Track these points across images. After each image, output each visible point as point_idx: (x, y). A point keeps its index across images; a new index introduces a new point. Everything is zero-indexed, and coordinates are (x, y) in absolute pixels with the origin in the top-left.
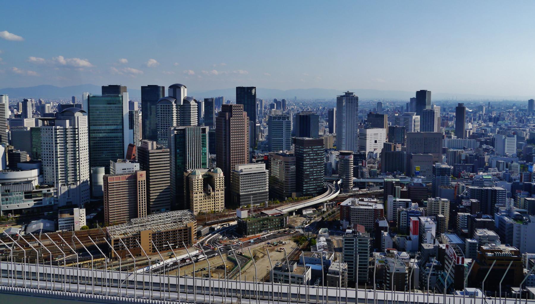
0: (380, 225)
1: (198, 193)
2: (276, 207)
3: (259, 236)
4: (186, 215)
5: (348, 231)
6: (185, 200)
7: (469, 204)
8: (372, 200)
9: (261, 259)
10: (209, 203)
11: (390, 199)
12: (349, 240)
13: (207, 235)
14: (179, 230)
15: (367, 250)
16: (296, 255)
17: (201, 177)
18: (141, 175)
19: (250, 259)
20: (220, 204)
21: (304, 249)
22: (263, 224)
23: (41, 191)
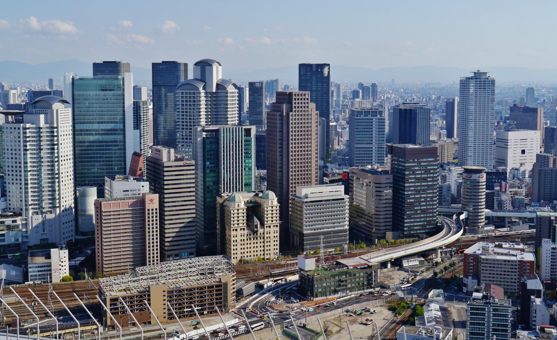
0: (529, 287)
2: (361, 254)
3: (333, 299)
4: (220, 264)
5: (475, 294)
6: (219, 240)
8: (516, 247)
9: (337, 336)
10: (255, 245)
12: (478, 309)
13: (251, 295)
14: (209, 287)
15: (506, 326)
16: (392, 330)
17: (242, 205)
18: (151, 201)
19: (318, 334)
20: (272, 248)
21: (404, 323)
22: (340, 281)
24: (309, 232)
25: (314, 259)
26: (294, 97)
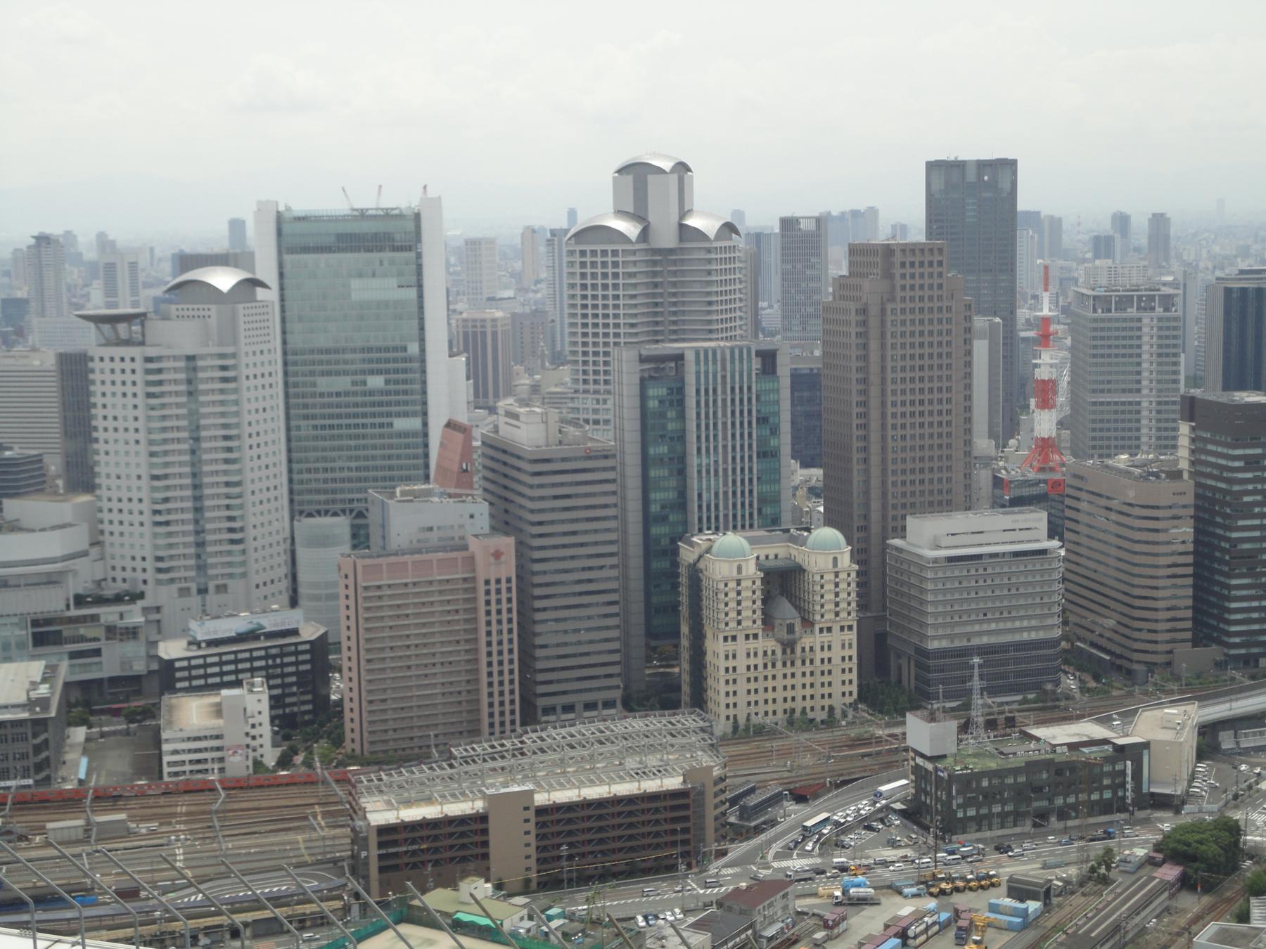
1: (741, 638)
6: (686, 666)
10: (789, 682)
17: (751, 569)
18: (497, 555)
20: (837, 689)
23: (95, 618)
24: (945, 644)
25: (953, 725)
26: (898, 258)
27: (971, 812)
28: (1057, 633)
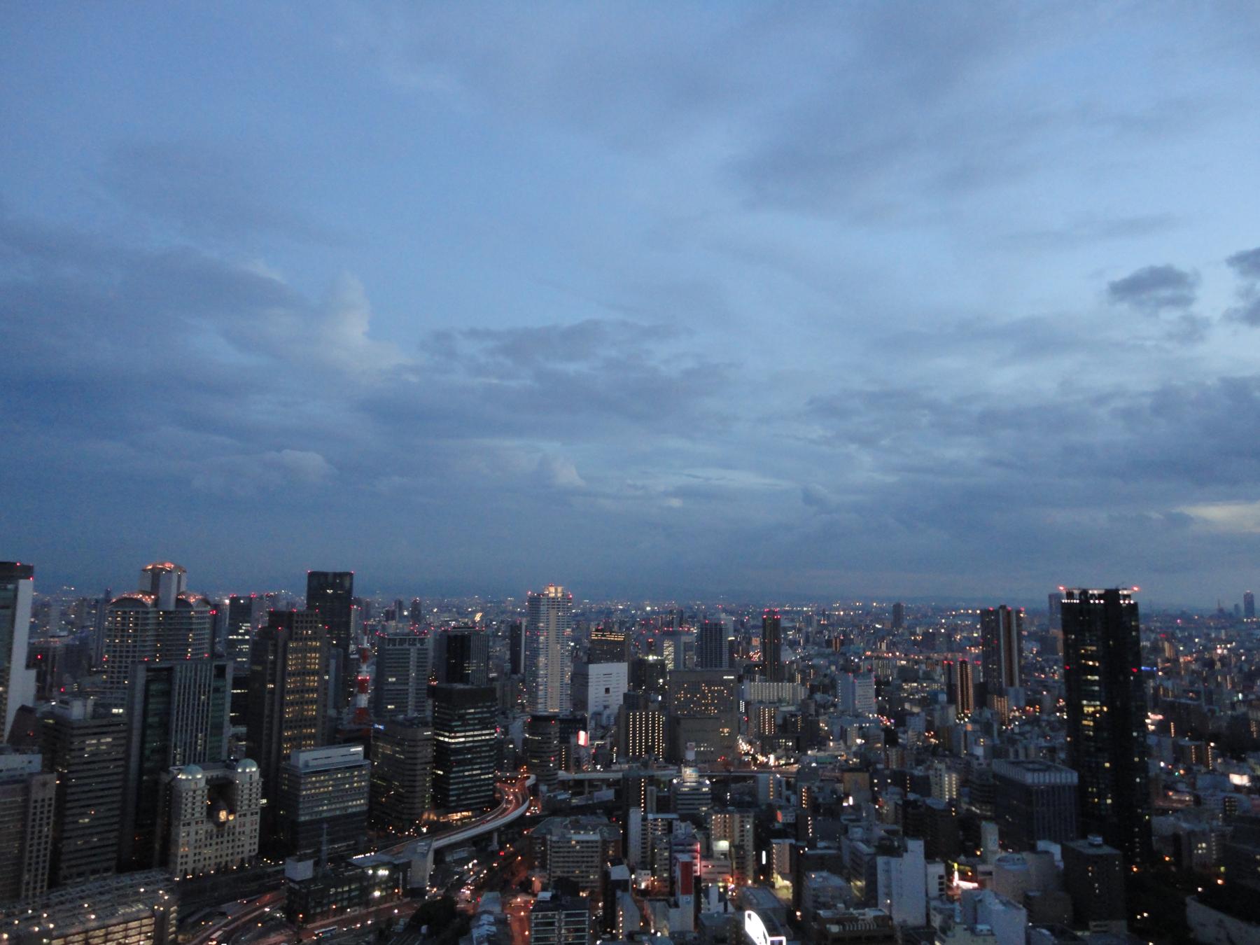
1: (193, 823)
7: (791, 819)
11: (635, 816)
17: (203, 783)
18: (44, 784)
24: (307, 818)
25: (310, 863)
26: (295, 618)
27: (319, 910)
28: (365, 808)
